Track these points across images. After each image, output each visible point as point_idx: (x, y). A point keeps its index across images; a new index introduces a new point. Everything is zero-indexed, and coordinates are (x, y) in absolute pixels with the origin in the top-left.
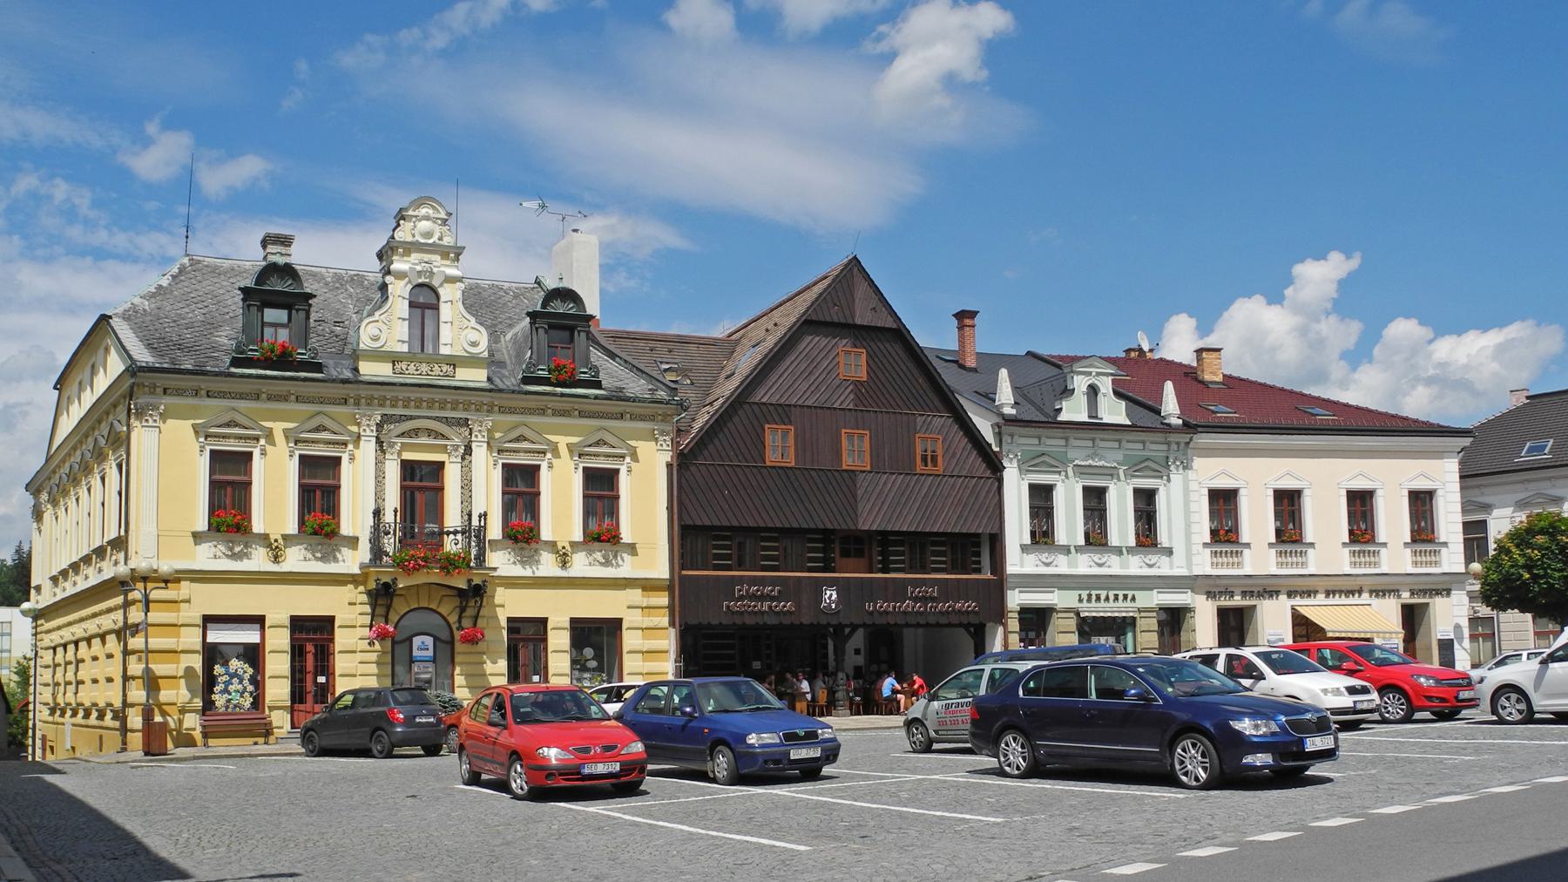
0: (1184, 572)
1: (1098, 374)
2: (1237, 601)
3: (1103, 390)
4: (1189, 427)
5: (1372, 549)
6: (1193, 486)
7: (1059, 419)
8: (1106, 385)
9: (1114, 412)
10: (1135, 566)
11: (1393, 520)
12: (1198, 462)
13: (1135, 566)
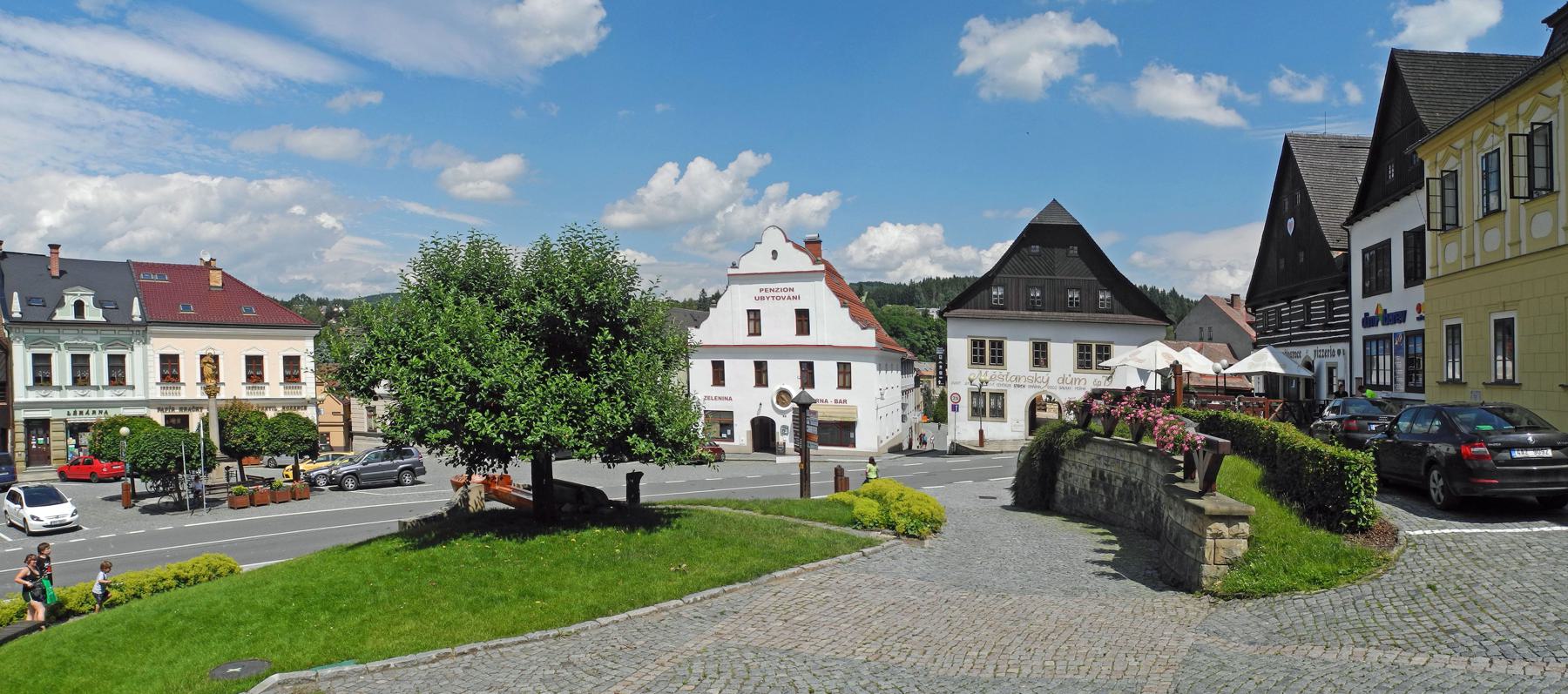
0: (143, 398)
1: (82, 295)
2: (177, 412)
3: (86, 303)
4: (146, 323)
5: (260, 386)
6: (150, 353)
7: (54, 319)
8: (88, 301)
9: (93, 314)
10: (108, 395)
11: (273, 371)
12: (153, 340)
13: (108, 395)
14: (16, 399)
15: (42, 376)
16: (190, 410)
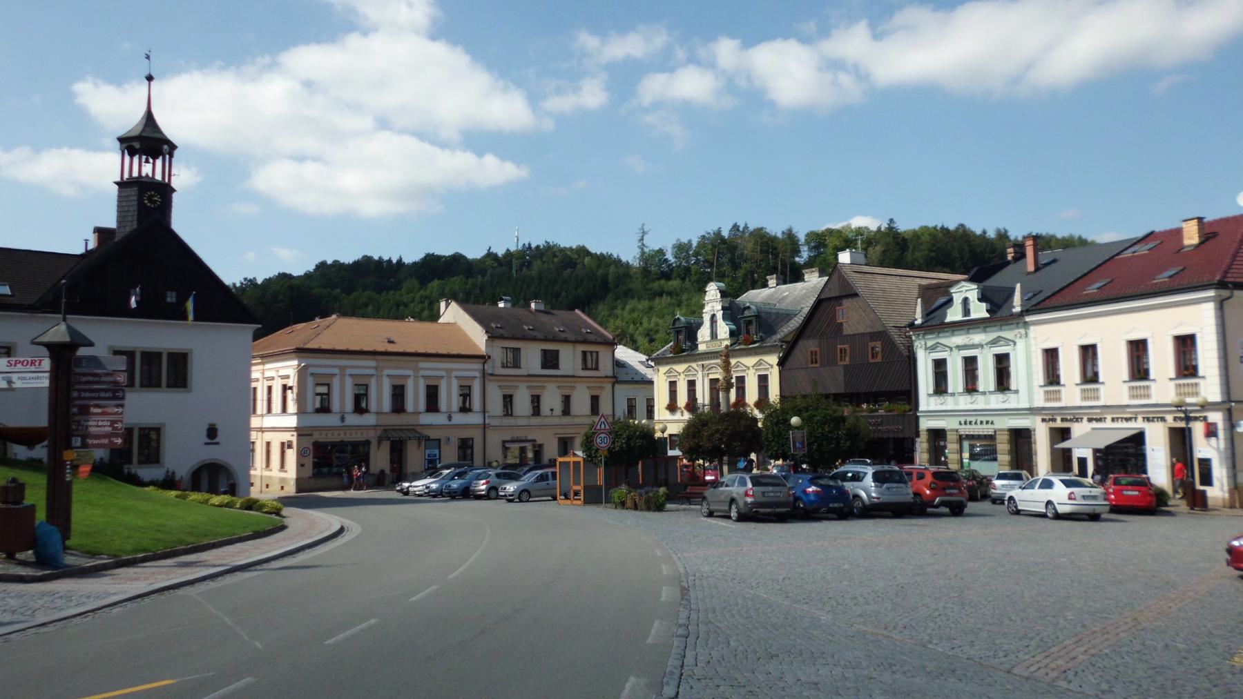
0: (1027, 405)
4: (1026, 312)
6: (1033, 348)
7: (946, 321)
11: (1162, 360)
14: (921, 409)
15: (940, 386)
16: (1071, 420)
